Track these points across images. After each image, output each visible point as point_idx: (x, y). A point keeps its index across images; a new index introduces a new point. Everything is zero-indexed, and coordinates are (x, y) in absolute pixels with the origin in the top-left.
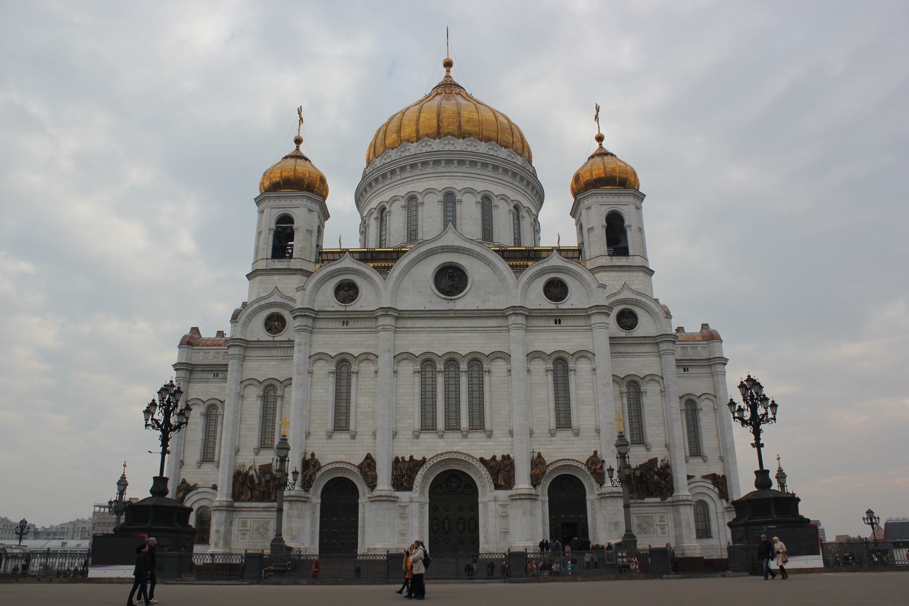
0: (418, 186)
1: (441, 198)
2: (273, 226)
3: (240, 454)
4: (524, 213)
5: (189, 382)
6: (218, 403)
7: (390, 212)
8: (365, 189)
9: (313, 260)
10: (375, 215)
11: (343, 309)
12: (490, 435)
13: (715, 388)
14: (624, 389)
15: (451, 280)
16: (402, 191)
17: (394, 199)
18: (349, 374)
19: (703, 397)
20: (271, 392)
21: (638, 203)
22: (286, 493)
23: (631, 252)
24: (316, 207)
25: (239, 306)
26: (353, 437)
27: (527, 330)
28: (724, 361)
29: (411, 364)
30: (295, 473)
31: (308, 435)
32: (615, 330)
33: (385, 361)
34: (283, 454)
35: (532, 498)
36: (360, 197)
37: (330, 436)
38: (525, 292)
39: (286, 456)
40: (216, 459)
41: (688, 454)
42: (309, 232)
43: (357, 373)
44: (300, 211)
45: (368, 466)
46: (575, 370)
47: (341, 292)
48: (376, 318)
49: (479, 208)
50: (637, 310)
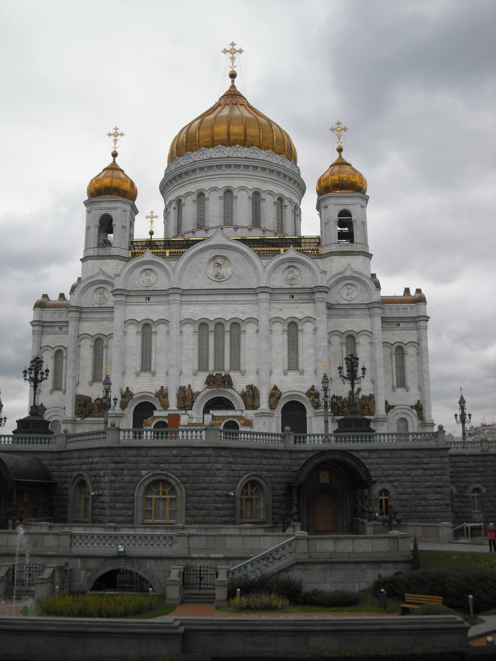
1: (221, 194)
2: (98, 224)
3: (79, 385)
4: (286, 203)
5: (42, 334)
6: (62, 348)
9: (127, 248)
10: (174, 205)
12: (243, 375)
13: (419, 339)
14: (344, 341)
16: (193, 188)
17: (188, 194)
18: (151, 333)
19: (409, 345)
20: (99, 343)
21: (363, 203)
22: (110, 412)
23: (355, 241)
24: (128, 208)
25: (75, 281)
26: (154, 375)
27: (270, 301)
28: (426, 319)
29: (192, 326)
30: (115, 399)
31: (124, 373)
34: (107, 387)
35: (270, 415)
37: (138, 375)
39: (109, 389)
40: (63, 388)
41: (395, 384)
42: (124, 227)
43: (156, 333)
44: (117, 209)
45: (162, 394)
46: (302, 330)
48: (168, 295)
49: (250, 202)
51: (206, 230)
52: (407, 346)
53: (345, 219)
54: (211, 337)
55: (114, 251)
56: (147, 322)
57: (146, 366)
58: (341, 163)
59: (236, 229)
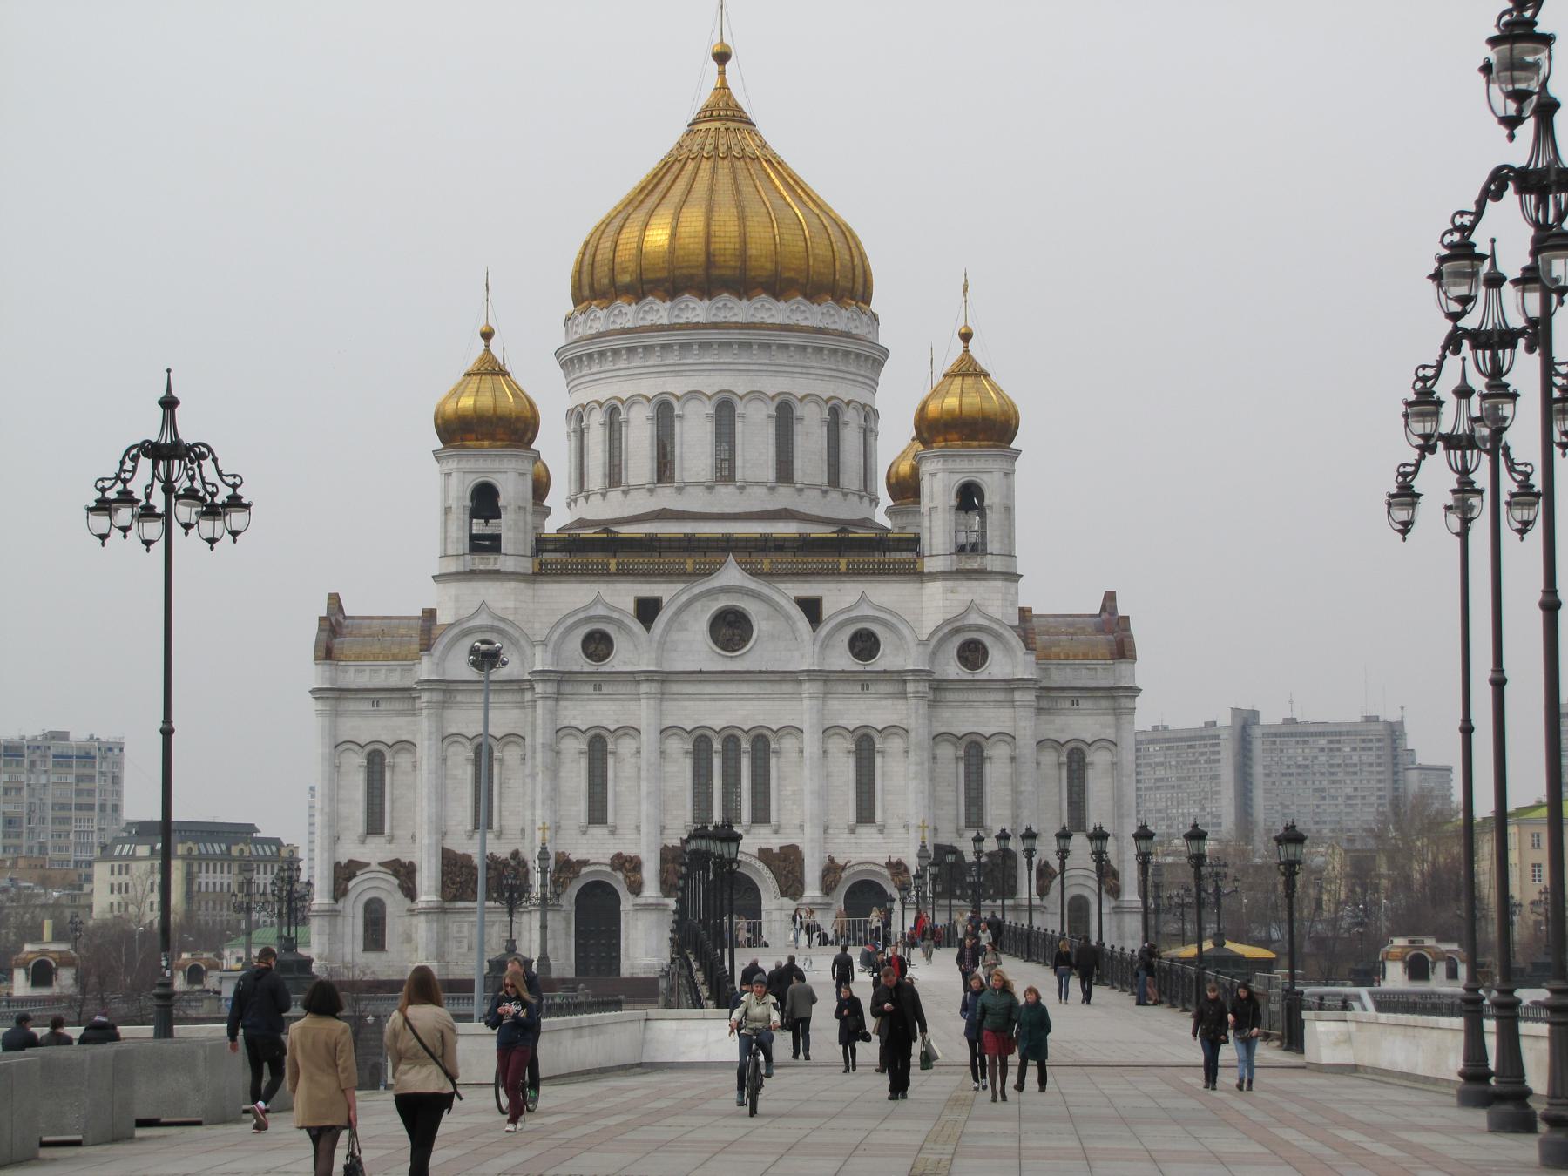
0: (676, 385)
2: (468, 503)
7: (627, 422)
8: (580, 358)
11: (593, 669)
14: (961, 753)
15: (731, 628)
16: (651, 386)
17: (634, 400)
21: (1005, 465)
24: (527, 466)
28: (1134, 691)
31: (558, 828)
32: (953, 669)
33: (649, 738)
36: (571, 361)
38: (825, 645)
47: (592, 648)
50: (987, 640)
51: (680, 490)
52: (1093, 748)
53: (969, 497)
54: (717, 762)
55: (506, 563)
56: (598, 731)
57: (597, 813)
58: (968, 370)
59: (742, 488)
